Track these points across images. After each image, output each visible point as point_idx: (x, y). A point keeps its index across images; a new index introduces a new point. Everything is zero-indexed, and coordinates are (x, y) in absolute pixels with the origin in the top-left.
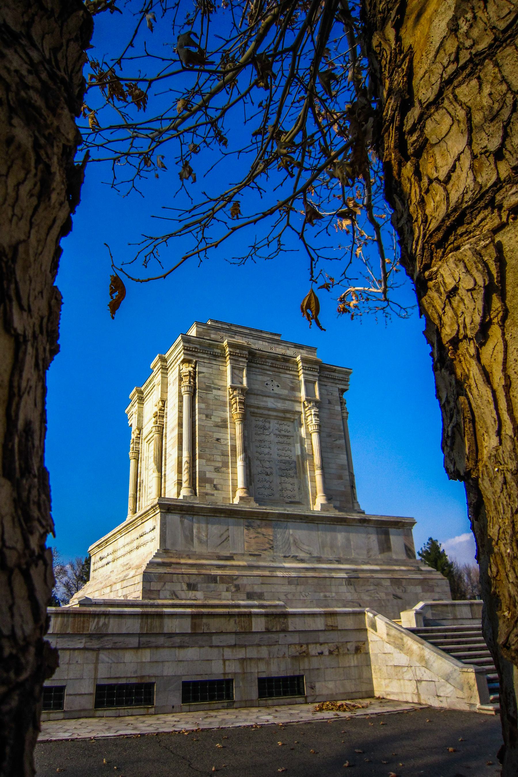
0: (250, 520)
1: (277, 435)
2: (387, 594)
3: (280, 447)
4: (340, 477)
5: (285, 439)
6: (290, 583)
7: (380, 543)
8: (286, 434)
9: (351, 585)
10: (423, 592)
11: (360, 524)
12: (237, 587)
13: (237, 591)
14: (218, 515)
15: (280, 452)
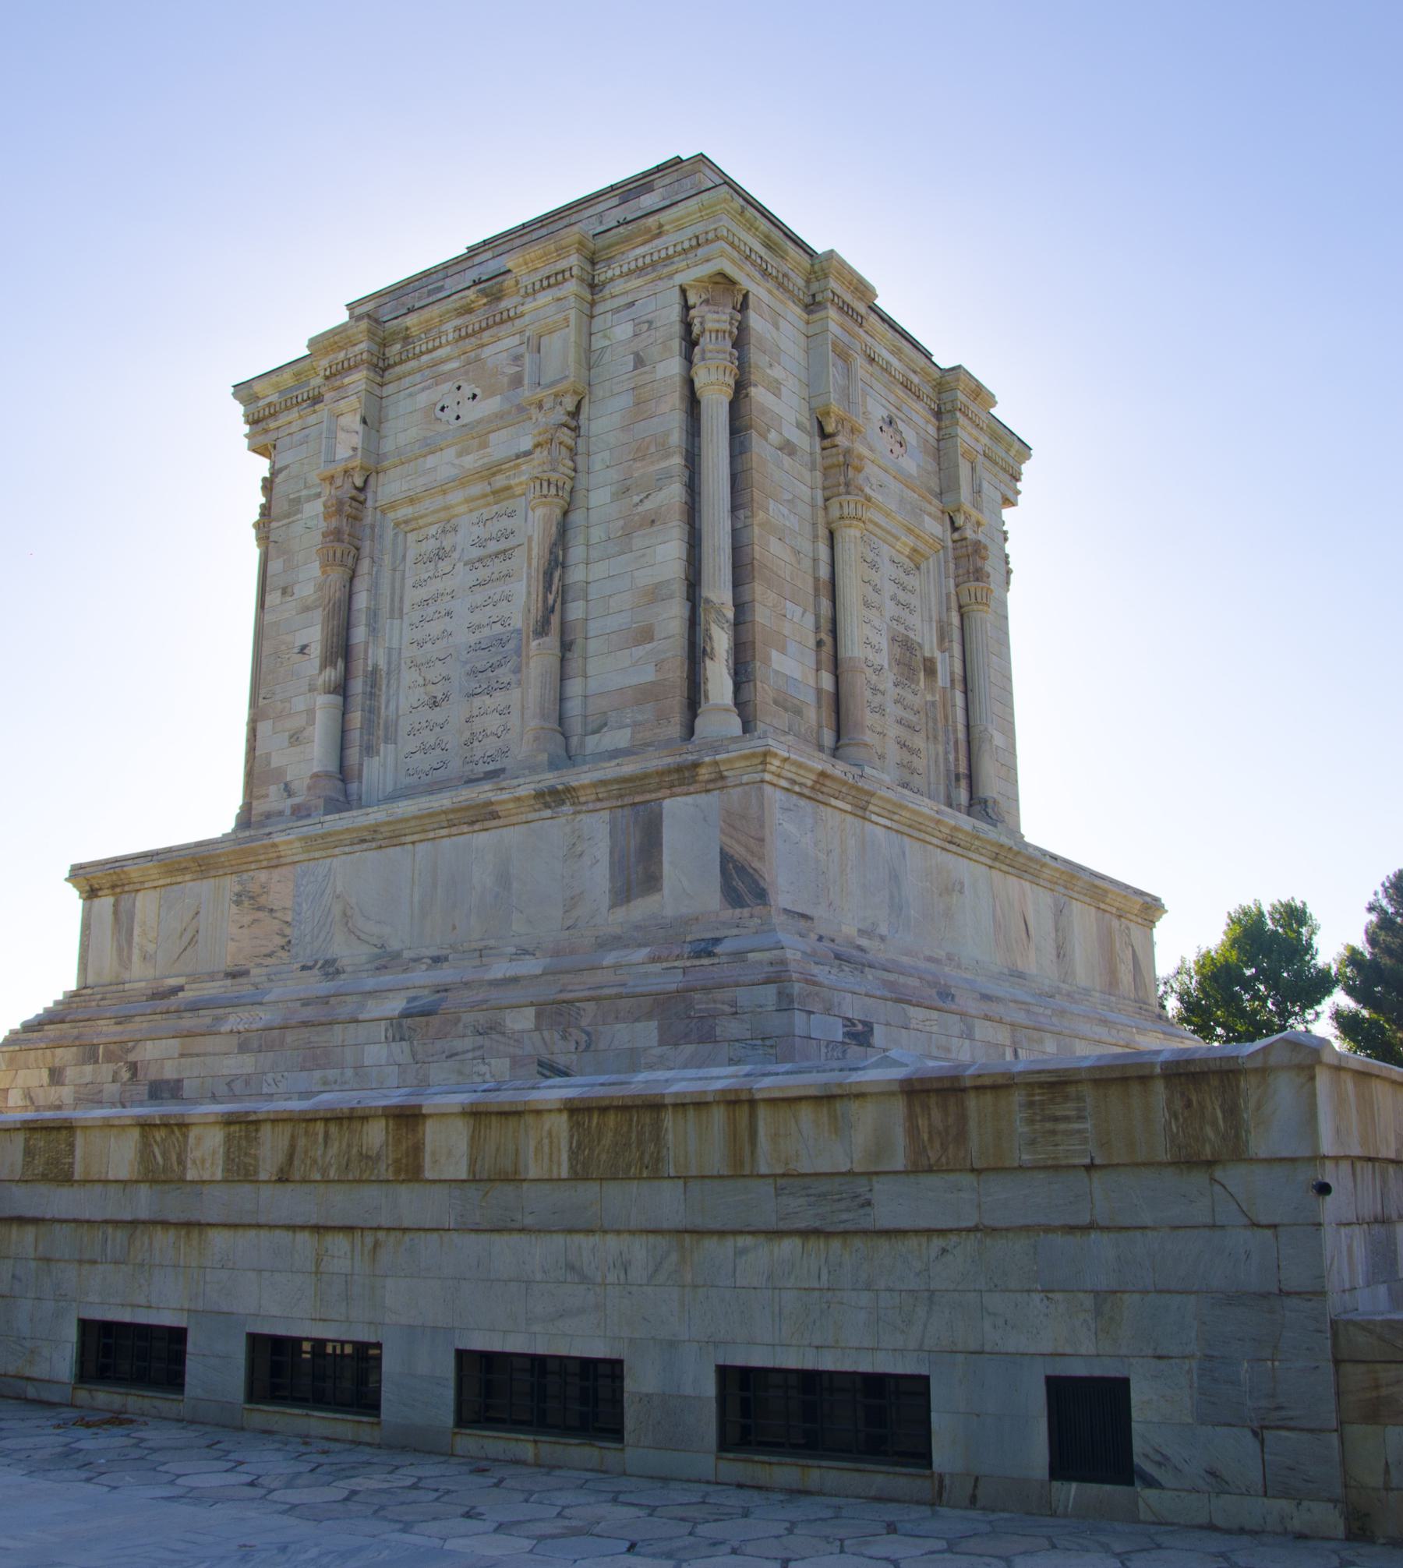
0: (245, 876)
1: (471, 564)
2: (515, 1062)
3: (479, 598)
4: (646, 635)
5: (499, 566)
6: (243, 1048)
7: (618, 865)
8: (504, 545)
9: (402, 1039)
10: (662, 1042)
11: (548, 813)
12: (133, 1067)
13: (131, 1079)
14: (179, 879)
15: (477, 618)
